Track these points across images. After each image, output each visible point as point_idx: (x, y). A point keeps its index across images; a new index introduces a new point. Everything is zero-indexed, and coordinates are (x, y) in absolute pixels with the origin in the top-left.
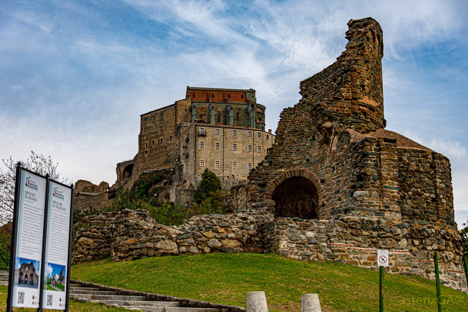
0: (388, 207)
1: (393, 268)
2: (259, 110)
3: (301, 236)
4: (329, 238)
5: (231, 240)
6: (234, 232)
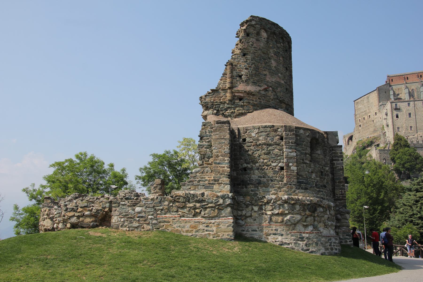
0: (218, 180)
1: (214, 234)
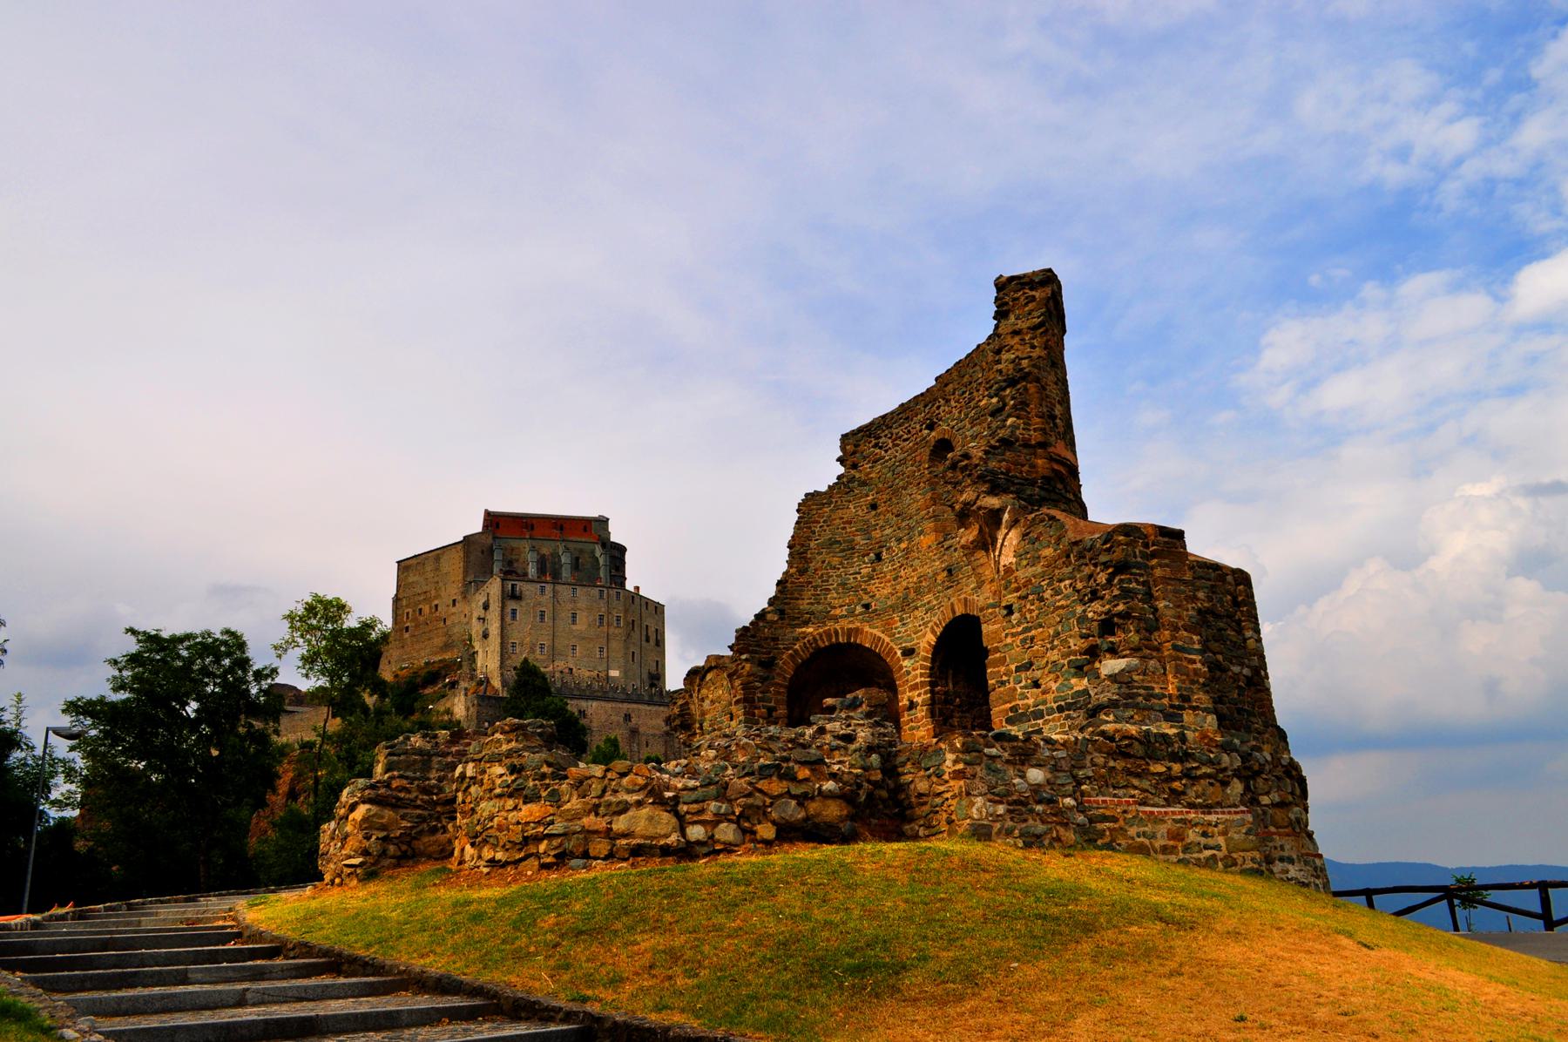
2: (617, 554)
3: (1017, 781)
4: (1079, 783)
5: (829, 802)
6: (833, 776)
